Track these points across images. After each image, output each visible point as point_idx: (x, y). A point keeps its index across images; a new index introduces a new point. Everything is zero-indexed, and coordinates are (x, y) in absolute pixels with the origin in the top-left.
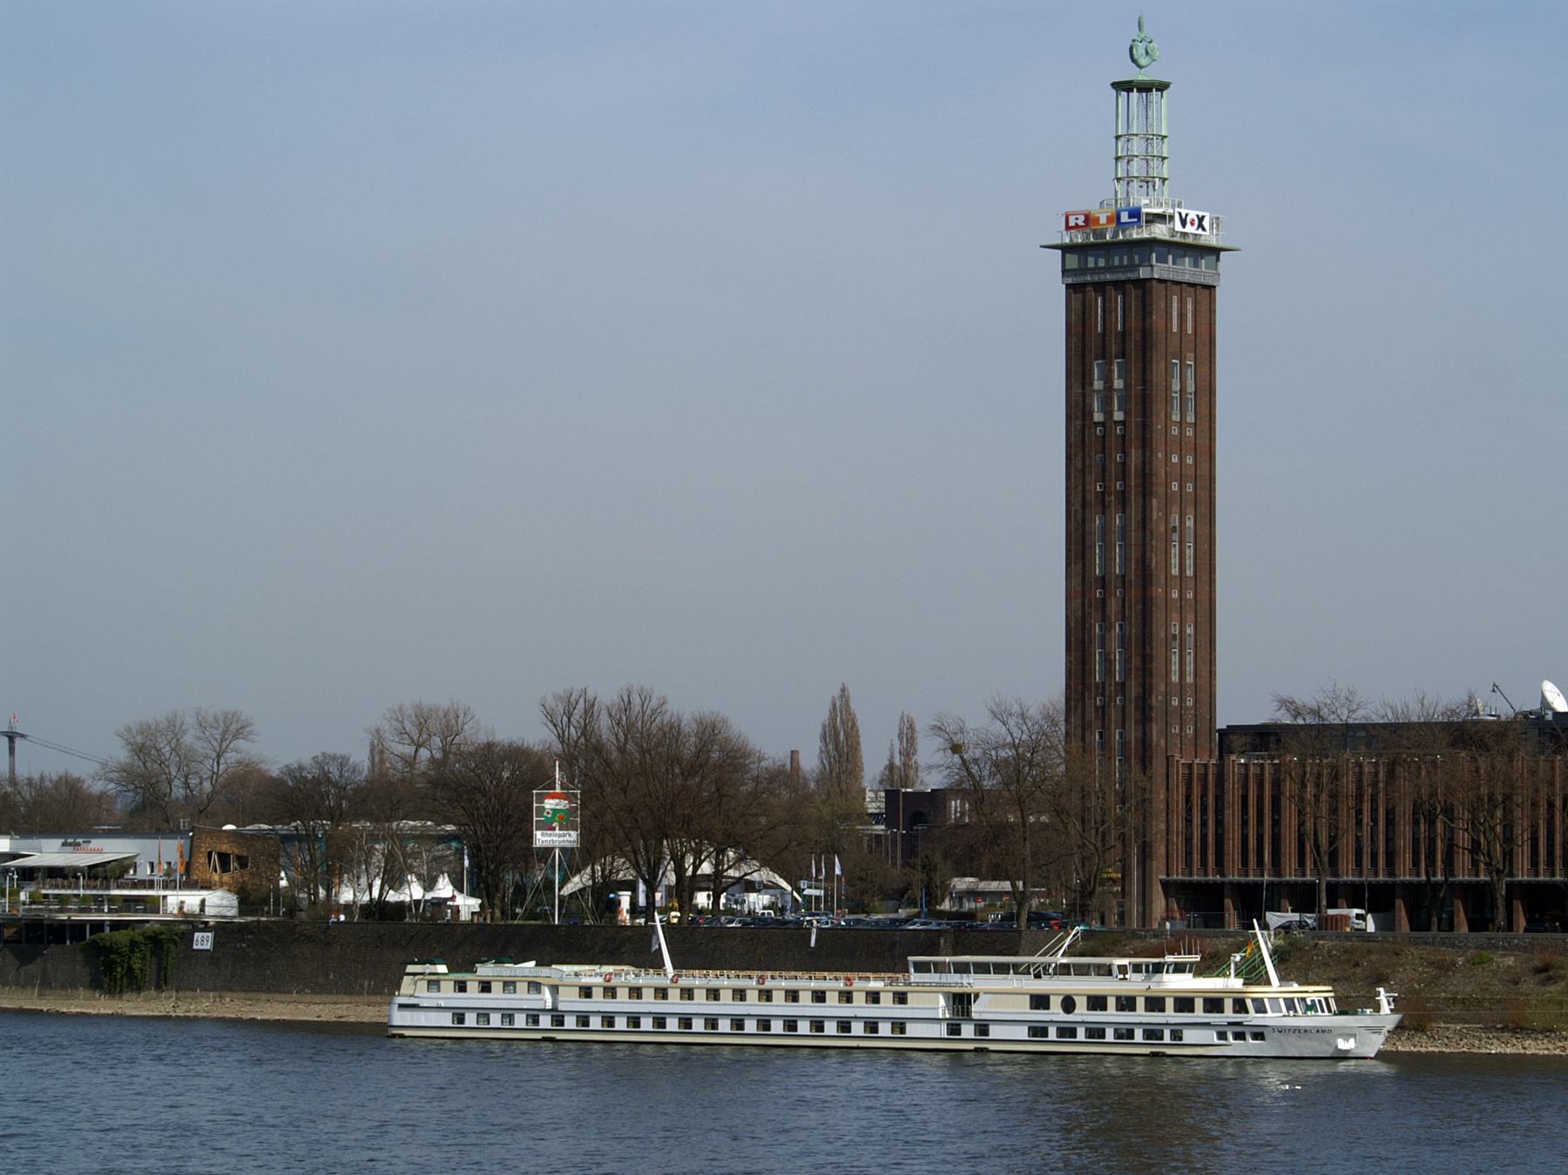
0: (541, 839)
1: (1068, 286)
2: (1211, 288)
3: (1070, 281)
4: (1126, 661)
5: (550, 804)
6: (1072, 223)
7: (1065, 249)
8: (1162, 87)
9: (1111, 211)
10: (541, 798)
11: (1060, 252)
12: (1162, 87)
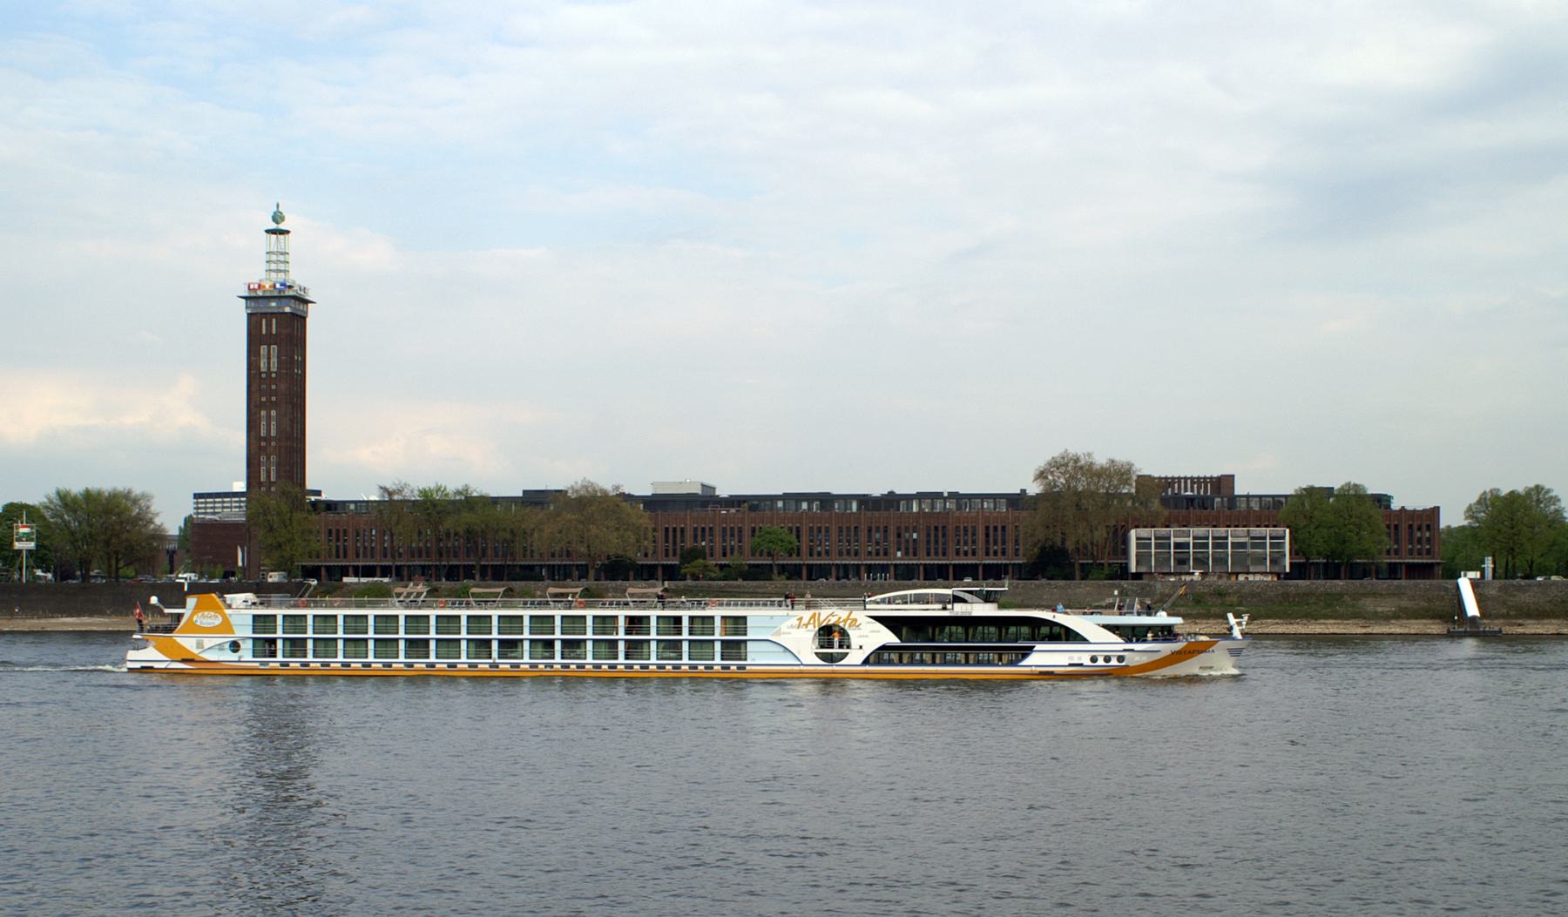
0: (17, 545)
1: (248, 314)
2: (304, 318)
3: (249, 312)
4: (278, 472)
5: (23, 530)
6: (252, 287)
7: (246, 298)
8: (288, 232)
9: (272, 283)
10: (18, 528)
11: (244, 301)
12: (288, 232)
